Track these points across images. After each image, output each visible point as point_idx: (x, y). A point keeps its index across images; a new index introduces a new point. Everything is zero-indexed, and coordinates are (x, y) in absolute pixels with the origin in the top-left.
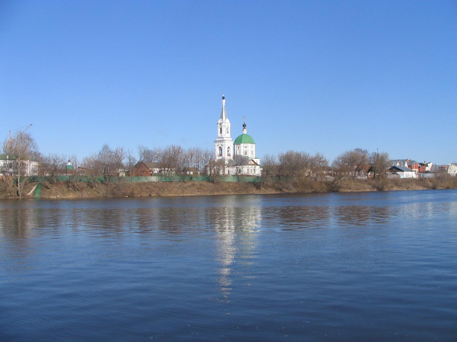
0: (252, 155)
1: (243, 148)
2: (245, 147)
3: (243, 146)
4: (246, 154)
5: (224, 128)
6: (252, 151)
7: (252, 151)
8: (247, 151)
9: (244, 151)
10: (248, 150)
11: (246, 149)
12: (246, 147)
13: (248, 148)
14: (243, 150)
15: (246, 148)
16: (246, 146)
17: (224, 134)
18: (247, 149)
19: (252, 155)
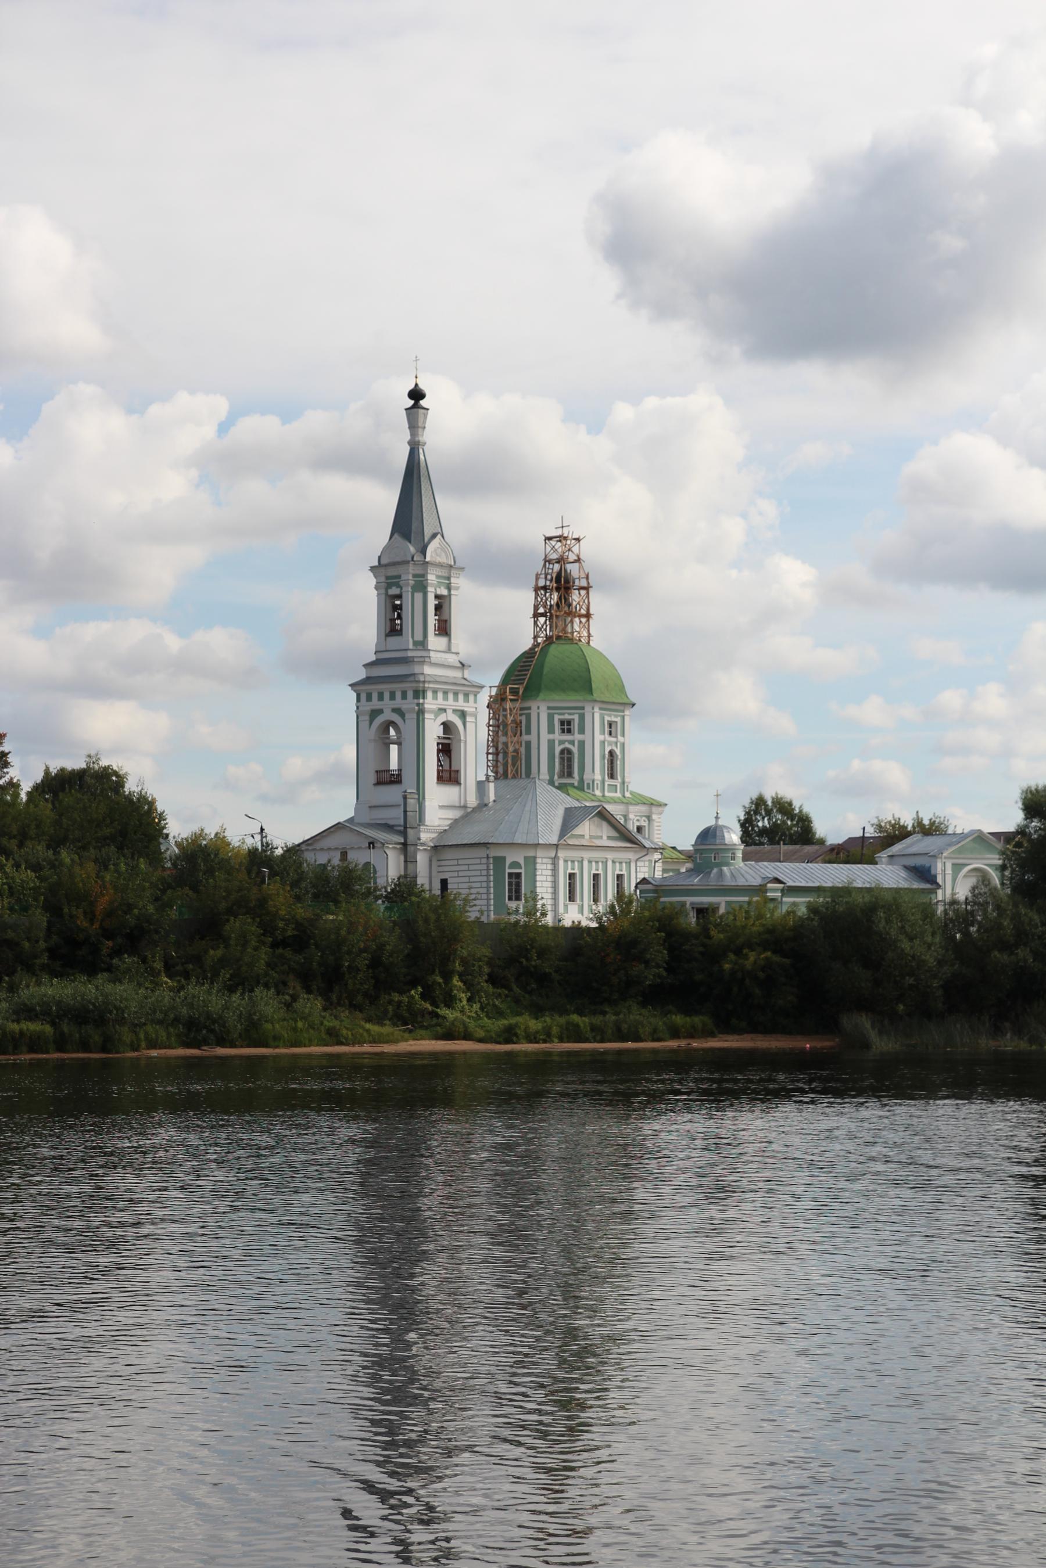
0: (612, 776)
1: (551, 730)
2: (562, 723)
3: (551, 718)
4: (570, 775)
5: (418, 596)
6: (607, 749)
7: (611, 753)
8: (575, 750)
9: (558, 749)
10: (582, 744)
11: (567, 737)
12: (569, 723)
13: (582, 731)
14: (551, 744)
15: (569, 731)
16: (567, 717)
17: (419, 637)
18: (577, 737)
19: (612, 776)
